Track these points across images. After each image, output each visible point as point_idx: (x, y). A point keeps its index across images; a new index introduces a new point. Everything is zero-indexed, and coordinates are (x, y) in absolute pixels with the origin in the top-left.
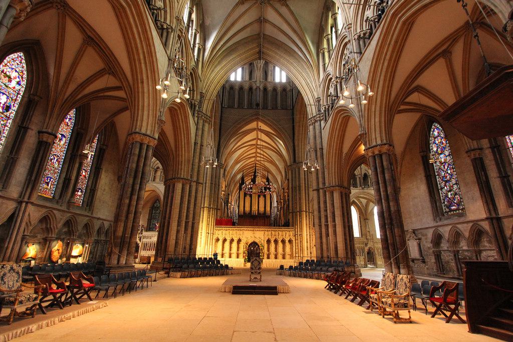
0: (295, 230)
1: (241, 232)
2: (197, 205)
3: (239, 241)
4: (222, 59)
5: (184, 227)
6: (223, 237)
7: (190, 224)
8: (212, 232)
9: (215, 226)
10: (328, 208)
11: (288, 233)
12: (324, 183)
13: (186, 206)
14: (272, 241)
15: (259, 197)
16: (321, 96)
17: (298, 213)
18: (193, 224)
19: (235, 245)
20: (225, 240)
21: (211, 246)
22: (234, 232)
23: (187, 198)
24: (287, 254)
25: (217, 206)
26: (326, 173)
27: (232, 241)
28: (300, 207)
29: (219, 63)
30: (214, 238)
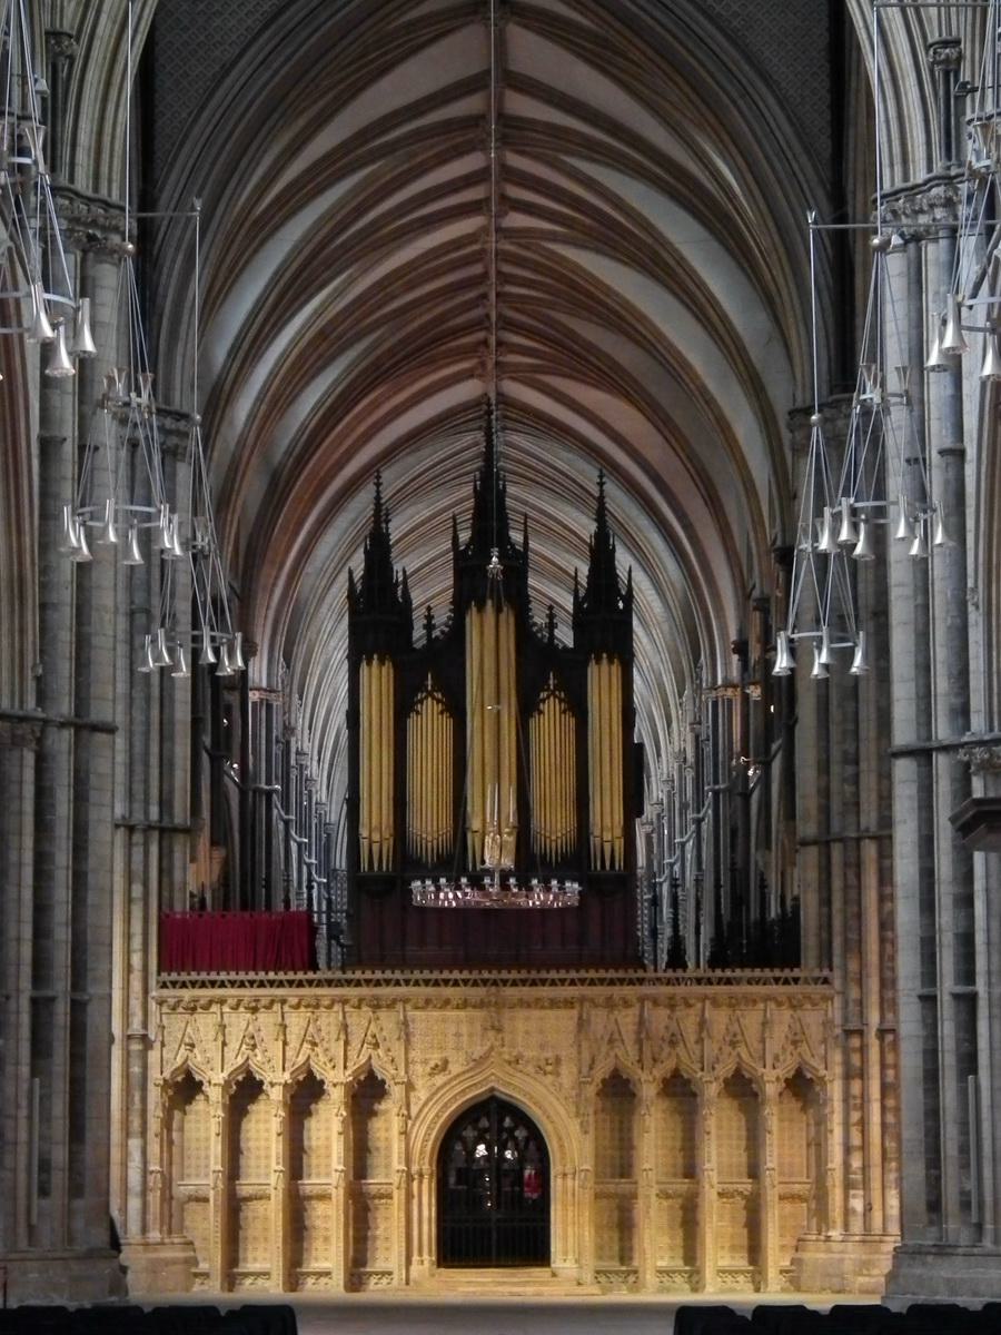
0: (844, 993)
1: (388, 1021)
2: (91, 879)
3: (367, 1094)
5: (25, 1032)
6: (235, 1061)
7: (62, 1011)
8: (136, 1027)
9: (154, 994)
10: (979, 885)
11: (783, 1018)
12: (962, 712)
13: (27, 894)
14: (648, 1090)
15: (527, 709)
17: (870, 850)
19: (328, 1127)
20: (246, 1090)
21: (135, 1144)
22: (329, 1021)
23: (28, 842)
24: (771, 1195)
25: (165, 804)
27: (306, 1092)
28: (886, 800)
30: (155, 1075)
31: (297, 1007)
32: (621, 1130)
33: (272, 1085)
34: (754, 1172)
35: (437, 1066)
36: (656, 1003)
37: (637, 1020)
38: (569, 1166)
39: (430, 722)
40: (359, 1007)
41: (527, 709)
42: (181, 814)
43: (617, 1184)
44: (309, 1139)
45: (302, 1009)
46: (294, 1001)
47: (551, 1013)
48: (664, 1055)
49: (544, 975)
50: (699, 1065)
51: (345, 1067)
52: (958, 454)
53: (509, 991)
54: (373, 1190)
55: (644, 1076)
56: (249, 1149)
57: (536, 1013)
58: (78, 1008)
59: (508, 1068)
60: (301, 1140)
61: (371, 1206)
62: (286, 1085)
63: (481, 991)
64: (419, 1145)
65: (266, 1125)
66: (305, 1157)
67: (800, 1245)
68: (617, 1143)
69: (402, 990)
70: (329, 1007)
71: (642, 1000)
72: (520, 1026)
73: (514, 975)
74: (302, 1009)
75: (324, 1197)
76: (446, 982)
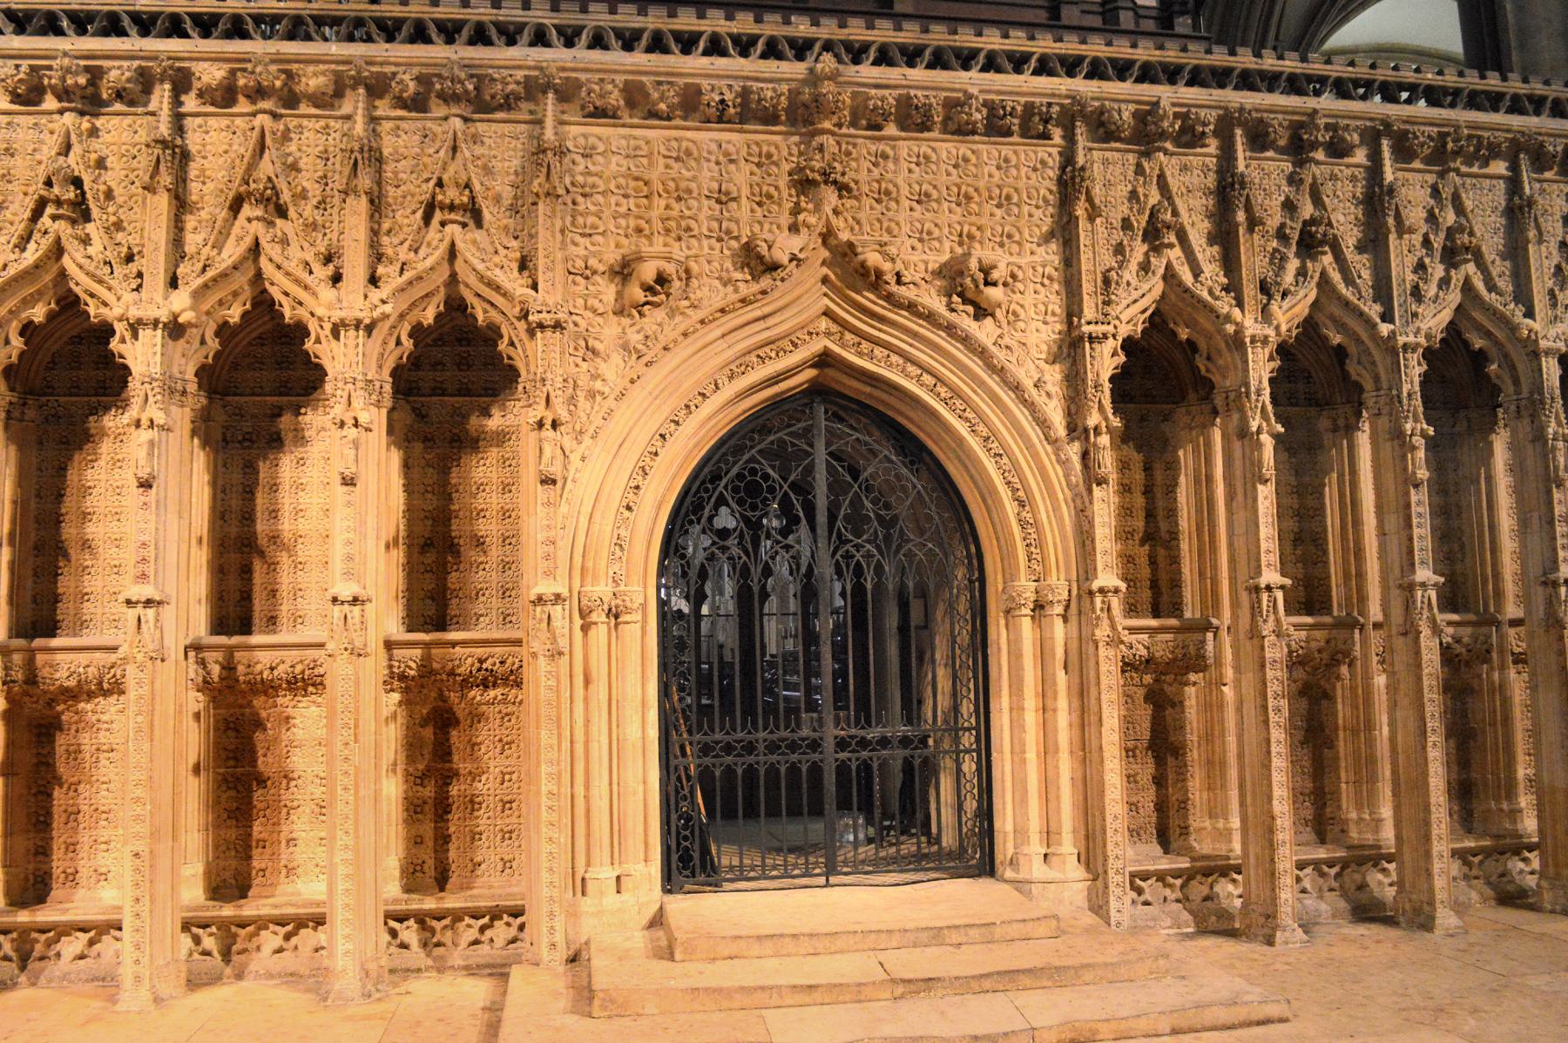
31: (225, 96)
32: (1148, 491)
33: (135, 328)
35: (662, 279)
36: (1259, 139)
37: (1211, 181)
38: (1053, 580)
40: (417, 104)
43: (1153, 631)
44: (274, 514)
45: (243, 106)
46: (211, 74)
47: (987, 151)
48: (1289, 278)
49: (966, 38)
50: (1378, 308)
51: (374, 281)
53: (868, 72)
54: (466, 660)
55: (1251, 325)
56: (86, 545)
57: (948, 148)
59: (867, 299)
60: (248, 517)
61: (461, 710)
62: (175, 329)
63: (793, 70)
64: (605, 527)
66: (258, 566)
68: (1139, 524)
69: (555, 56)
70: (326, 101)
71: (1226, 123)
72: (903, 178)
73: (884, 33)
74: (243, 106)
75: (306, 683)
76: (687, 43)
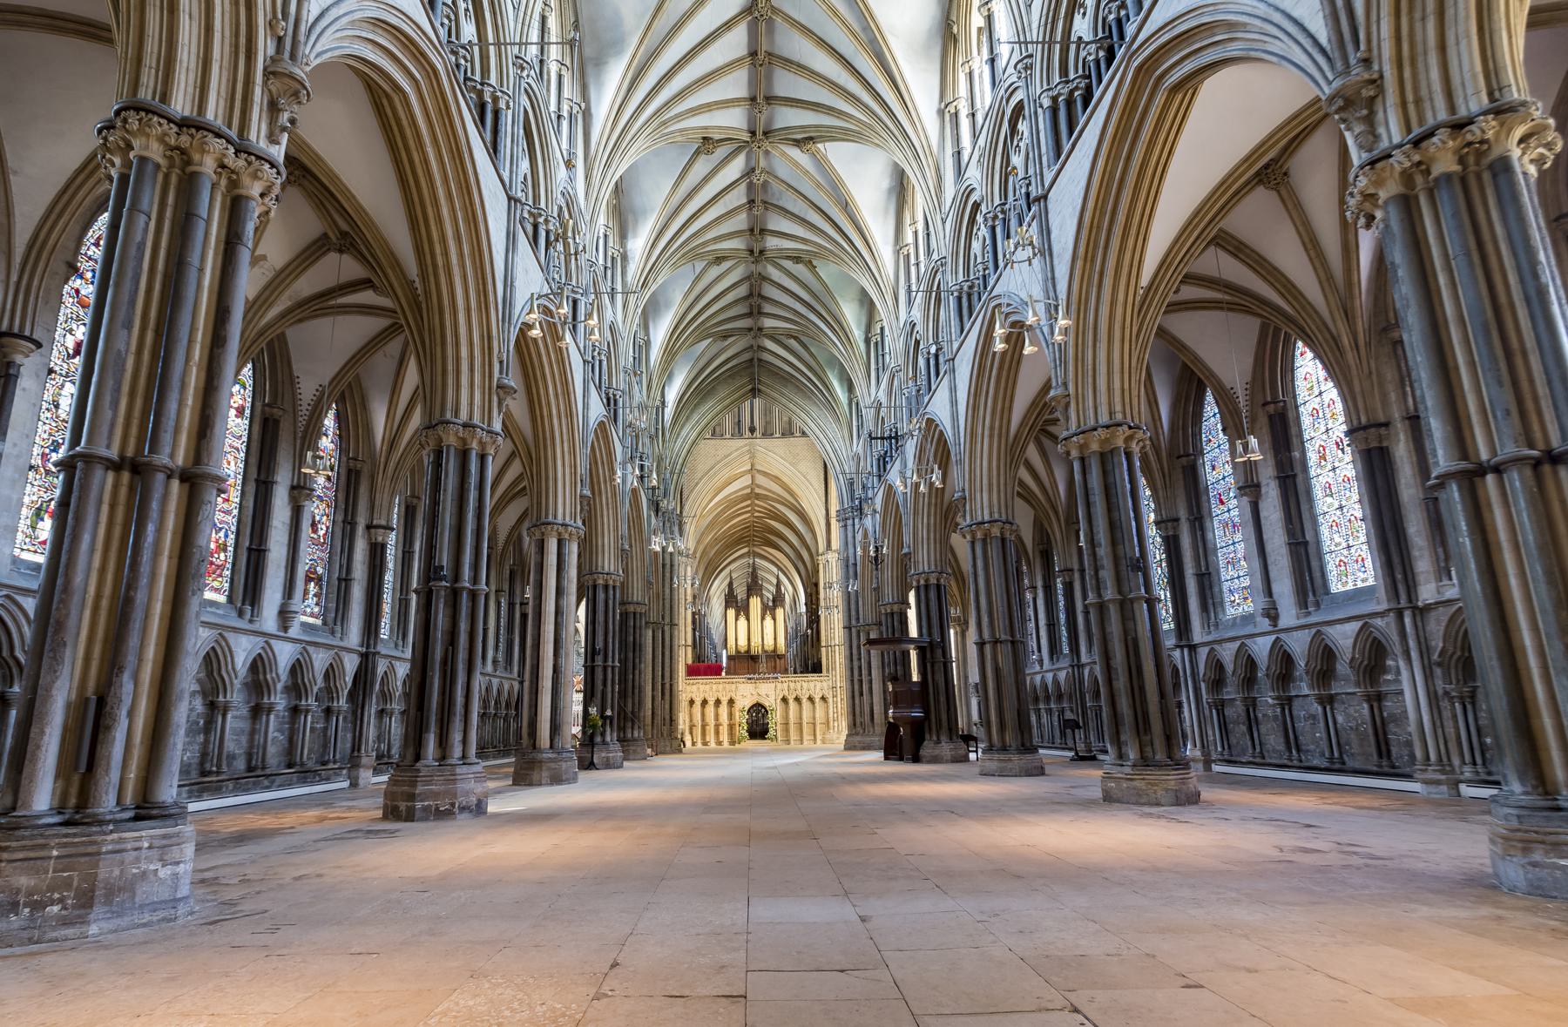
1: (734, 686)
3: (731, 702)
4: (692, 411)
6: (702, 696)
7: (668, 686)
11: (818, 685)
12: (858, 619)
14: (791, 701)
15: (763, 619)
16: (854, 476)
18: (671, 685)
22: (721, 686)
24: (818, 722)
26: (860, 603)
27: (718, 702)
29: (688, 419)
34: (814, 718)
39: (742, 621)
41: (763, 619)
42: (690, 642)
52: (855, 565)
58: (671, 685)
65: (710, 709)
67: (824, 734)
